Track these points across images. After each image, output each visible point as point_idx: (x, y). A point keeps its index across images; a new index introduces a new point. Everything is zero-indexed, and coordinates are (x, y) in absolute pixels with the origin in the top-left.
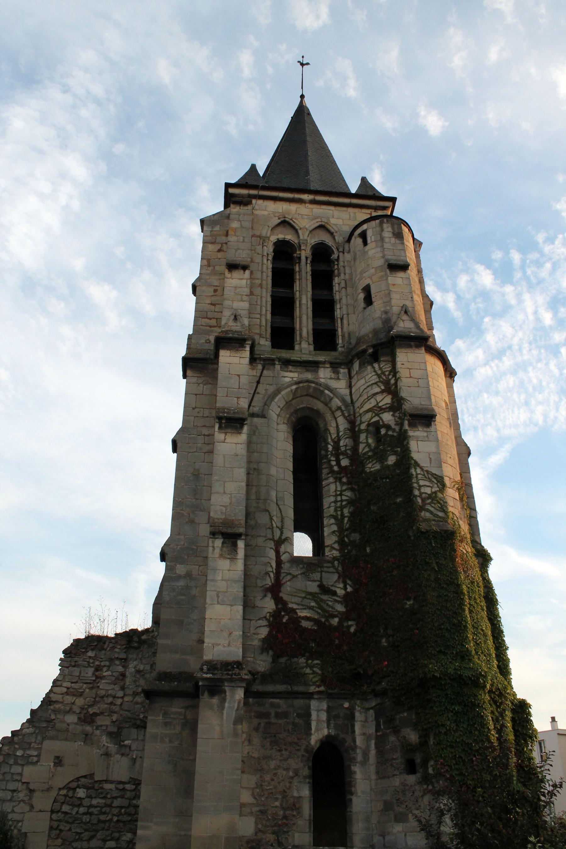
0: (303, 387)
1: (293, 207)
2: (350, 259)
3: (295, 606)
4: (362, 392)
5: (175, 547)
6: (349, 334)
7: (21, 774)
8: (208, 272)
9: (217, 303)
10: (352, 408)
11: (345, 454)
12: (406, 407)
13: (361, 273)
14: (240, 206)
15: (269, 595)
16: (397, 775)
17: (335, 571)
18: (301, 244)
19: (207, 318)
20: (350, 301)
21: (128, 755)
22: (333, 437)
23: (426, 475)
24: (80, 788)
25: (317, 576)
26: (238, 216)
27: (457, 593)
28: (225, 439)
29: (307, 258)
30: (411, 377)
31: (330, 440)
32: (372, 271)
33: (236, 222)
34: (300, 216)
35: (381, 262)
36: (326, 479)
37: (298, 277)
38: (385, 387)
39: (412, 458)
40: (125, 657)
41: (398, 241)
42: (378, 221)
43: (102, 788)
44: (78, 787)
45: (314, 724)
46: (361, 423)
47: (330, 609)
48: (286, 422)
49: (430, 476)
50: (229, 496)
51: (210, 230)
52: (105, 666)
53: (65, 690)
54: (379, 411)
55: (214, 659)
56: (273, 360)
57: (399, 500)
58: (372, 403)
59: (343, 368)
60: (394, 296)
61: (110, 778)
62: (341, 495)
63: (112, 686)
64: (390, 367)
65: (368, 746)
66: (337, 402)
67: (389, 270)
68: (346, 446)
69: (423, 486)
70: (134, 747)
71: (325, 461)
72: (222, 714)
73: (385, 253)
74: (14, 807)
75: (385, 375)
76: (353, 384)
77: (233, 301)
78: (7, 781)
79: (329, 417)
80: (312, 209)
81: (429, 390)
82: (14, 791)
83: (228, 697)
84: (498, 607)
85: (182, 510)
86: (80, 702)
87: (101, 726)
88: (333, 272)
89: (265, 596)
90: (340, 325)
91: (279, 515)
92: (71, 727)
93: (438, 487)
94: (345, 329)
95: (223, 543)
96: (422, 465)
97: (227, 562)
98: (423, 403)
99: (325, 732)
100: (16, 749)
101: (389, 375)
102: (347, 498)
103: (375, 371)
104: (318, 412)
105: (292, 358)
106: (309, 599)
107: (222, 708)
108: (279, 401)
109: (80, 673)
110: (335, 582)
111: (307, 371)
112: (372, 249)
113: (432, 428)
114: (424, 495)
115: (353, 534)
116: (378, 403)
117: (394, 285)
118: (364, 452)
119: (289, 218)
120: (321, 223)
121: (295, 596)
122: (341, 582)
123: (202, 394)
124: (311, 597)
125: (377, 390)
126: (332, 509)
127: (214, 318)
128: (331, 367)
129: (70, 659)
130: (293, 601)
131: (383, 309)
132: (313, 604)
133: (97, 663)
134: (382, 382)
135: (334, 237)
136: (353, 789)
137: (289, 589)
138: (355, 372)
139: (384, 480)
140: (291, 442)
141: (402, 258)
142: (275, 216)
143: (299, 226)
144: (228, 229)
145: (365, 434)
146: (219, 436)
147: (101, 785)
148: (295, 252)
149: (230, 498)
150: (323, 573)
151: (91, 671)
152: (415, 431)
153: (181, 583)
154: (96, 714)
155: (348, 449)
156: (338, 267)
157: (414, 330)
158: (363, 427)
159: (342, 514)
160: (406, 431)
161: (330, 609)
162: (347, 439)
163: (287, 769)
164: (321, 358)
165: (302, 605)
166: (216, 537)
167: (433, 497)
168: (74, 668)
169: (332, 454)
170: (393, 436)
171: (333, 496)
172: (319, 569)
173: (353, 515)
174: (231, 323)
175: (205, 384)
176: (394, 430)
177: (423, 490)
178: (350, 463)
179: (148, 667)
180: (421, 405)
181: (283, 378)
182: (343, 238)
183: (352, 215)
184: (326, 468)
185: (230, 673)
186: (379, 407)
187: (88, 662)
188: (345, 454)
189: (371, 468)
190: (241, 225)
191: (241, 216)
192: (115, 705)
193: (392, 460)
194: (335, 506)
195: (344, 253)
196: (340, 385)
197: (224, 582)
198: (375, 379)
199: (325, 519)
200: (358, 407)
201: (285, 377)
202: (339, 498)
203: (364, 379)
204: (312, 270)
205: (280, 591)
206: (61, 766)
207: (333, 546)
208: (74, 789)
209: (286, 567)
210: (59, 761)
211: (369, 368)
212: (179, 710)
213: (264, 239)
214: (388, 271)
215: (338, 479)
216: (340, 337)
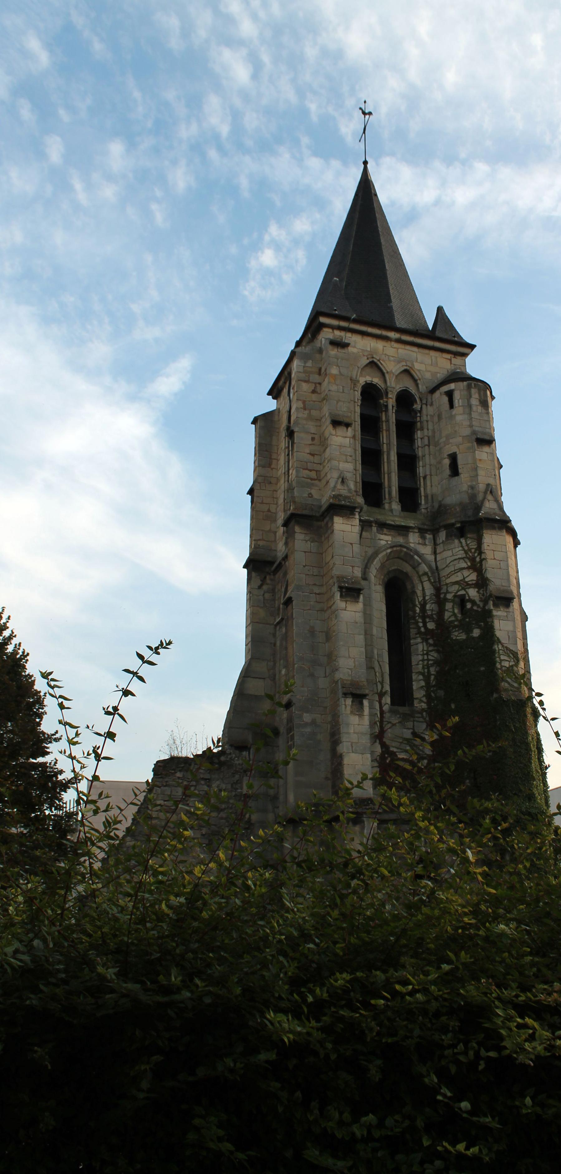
0: (396, 550)
1: (379, 345)
2: (432, 414)
3: (395, 750)
4: (449, 563)
5: (301, 698)
6: (432, 496)
8: (305, 416)
10: (437, 574)
11: (431, 617)
12: (491, 587)
13: (448, 437)
14: (338, 347)
15: (378, 741)
17: (423, 720)
18: (388, 391)
19: (307, 469)
20: (433, 462)
22: (420, 600)
23: (505, 650)
25: (410, 724)
26: (336, 360)
27: (527, 750)
28: (346, 607)
29: (393, 407)
30: (494, 559)
31: (417, 603)
32: (460, 439)
33: (335, 367)
34: (387, 357)
35: (467, 432)
36: (415, 638)
37: (384, 428)
38: (471, 564)
39: (496, 635)
40: (209, 777)
41: (484, 411)
42: (465, 383)
46: (448, 592)
47: (421, 753)
48: (381, 583)
49: (508, 652)
50: (353, 660)
51: (303, 365)
52: (192, 786)
54: (466, 586)
56: (371, 522)
57: (482, 669)
58: (458, 577)
59: (429, 534)
60: (481, 473)
62: (427, 654)
64: (475, 545)
66: (424, 568)
67: (477, 444)
68: (432, 610)
69: (503, 660)
71: (413, 621)
73: (474, 423)
75: (471, 552)
76: (438, 551)
77: (339, 461)
79: (416, 580)
80: (398, 349)
81: (508, 572)
84: (544, 754)
85: (303, 664)
88: (415, 423)
89: (375, 742)
90: (422, 484)
91: (380, 671)
93: (514, 661)
94: (429, 491)
95: (352, 702)
96: (503, 641)
97: (357, 718)
98: (504, 584)
101: (475, 552)
102: (433, 658)
103: (462, 546)
104: (406, 575)
105: (388, 522)
106: (405, 744)
108: (376, 563)
109: (171, 792)
110: (424, 730)
111: (399, 535)
112: (459, 415)
113: (511, 609)
114: (504, 668)
115: (439, 691)
116: (464, 578)
117: (480, 460)
118: (450, 620)
119: (376, 359)
120: (406, 368)
121: (395, 741)
122: (428, 729)
123: (311, 552)
124: (406, 742)
125: (464, 565)
126: (420, 666)
127: (314, 470)
128: (419, 532)
129: (161, 780)
130: (393, 745)
131: (469, 484)
132: (408, 748)
133: (185, 783)
134: (468, 559)
137: (389, 735)
138: (441, 541)
139: (470, 650)
140: (385, 602)
141: (487, 430)
142: (364, 356)
143: (386, 370)
144: (320, 366)
145: (451, 604)
146: (340, 603)
148: (382, 399)
149: (354, 662)
150: (415, 722)
152: (498, 611)
153: (308, 730)
155: (434, 614)
156: (420, 419)
157: (497, 511)
158: (450, 596)
159: (429, 671)
160: (490, 611)
161: (421, 753)
162: (433, 604)
164: (411, 523)
165: (401, 749)
166: (347, 696)
167: (510, 671)
168: (167, 788)
169: (419, 616)
170: (477, 611)
171: (421, 655)
172: (412, 719)
173: (438, 674)
174: (339, 486)
175: (312, 542)
176: (478, 606)
177: (503, 664)
178: (436, 627)
179: (229, 786)
180: (502, 586)
181: (379, 541)
182: (426, 387)
183: (434, 360)
184: (413, 628)
186: (466, 582)
188: (431, 617)
189: (457, 636)
190: (340, 372)
191: (339, 360)
193: (476, 633)
194: (423, 664)
195: (427, 405)
196: (426, 551)
198: (462, 554)
199: (413, 674)
200: (445, 576)
201: (381, 540)
202: (426, 657)
203: (451, 551)
204: (396, 420)
205: (384, 737)
207: (422, 699)
209: (387, 715)
211: (456, 541)
213: (354, 382)
214: (475, 444)
215: (425, 640)
216: (423, 498)
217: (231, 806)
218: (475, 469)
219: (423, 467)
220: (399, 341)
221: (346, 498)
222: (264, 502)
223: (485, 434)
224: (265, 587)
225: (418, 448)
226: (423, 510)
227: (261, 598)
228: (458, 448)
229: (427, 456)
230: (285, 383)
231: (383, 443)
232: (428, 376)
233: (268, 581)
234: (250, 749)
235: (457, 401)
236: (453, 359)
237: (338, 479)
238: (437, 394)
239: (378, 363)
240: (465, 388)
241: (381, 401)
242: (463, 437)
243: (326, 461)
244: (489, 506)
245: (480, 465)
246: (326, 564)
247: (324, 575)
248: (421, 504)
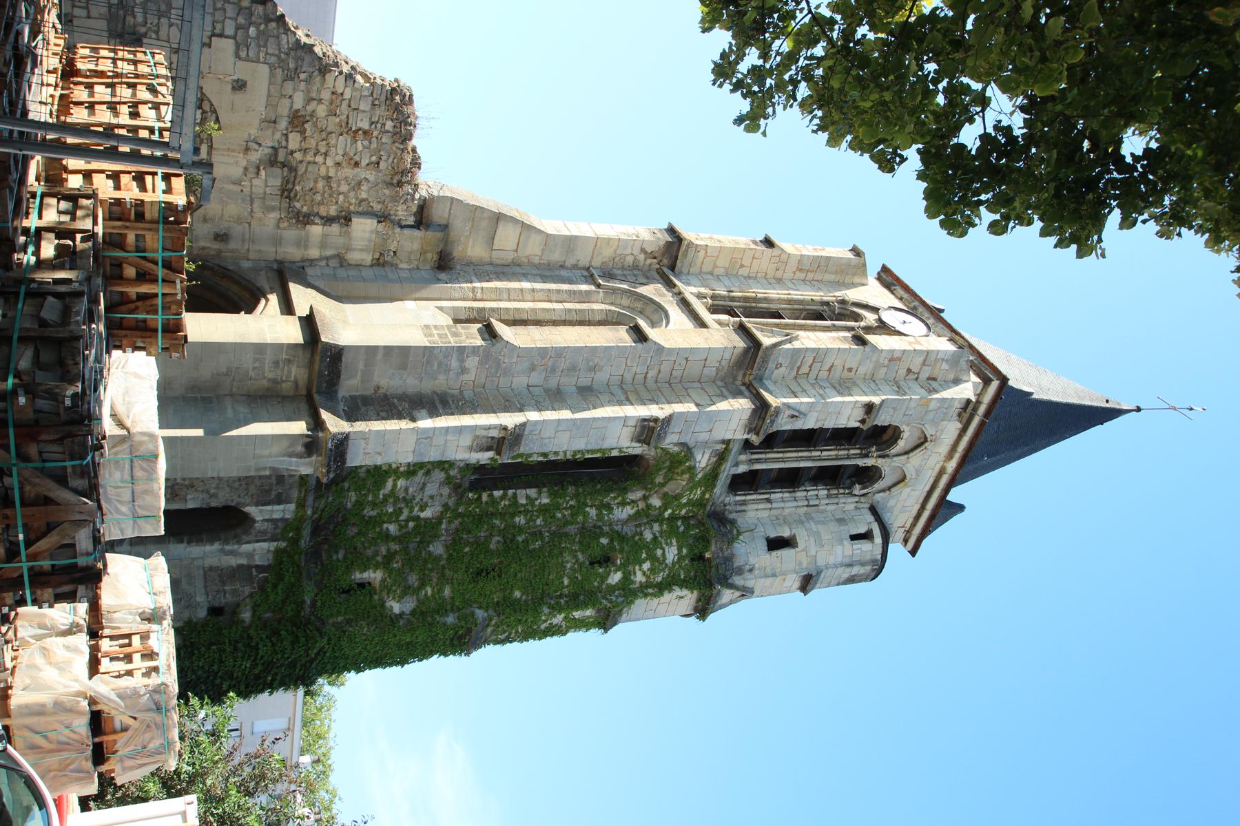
1: (944, 449)
6: (744, 511)
7: (221, 35)
9: (832, 373)
13: (817, 535)
16: (208, 597)
19: (814, 361)
20: (787, 512)
21: (246, 175)
24: (202, 114)
35: (821, 562)
41: (842, 580)
42: (879, 557)
44: (204, 112)
45: (269, 508)
53: (340, 91)
55: (349, 442)
60: (769, 581)
61: (214, 152)
63: (341, 152)
65: (240, 555)
70: (256, 182)
72: (284, 456)
78: (213, 15)
83: (303, 460)
85: (550, 357)
86: (321, 111)
87: (287, 140)
88: (837, 488)
92: (287, 102)
95: (493, 438)
99: (259, 518)
100: (257, 28)
107: (291, 455)
109: (364, 111)
117: (784, 580)
120: (908, 477)
131: (757, 566)
135: (883, 491)
136: (194, 544)
147: (205, 141)
148: (877, 450)
149: (549, 438)
151: (365, 125)
153: (454, 364)
154: (303, 132)
163: (217, 487)
175: (718, 369)
179: (364, 195)
185: (332, 463)
187: (378, 122)
192: (315, 155)
197: (443, 442)
201: (703, 455)
206: (234, 88)
210: (240, 86)
212: (293, 375)
217: (335, 196)
218: (774, 575)
219: (782, 498)
220: (942, 472)
221: (772, 422)
222: (754, 260)
223: (816, 583)
224: (642, 257)
225: (805, 490)
226: (728, 499)
227: (629, 251)
228: (803, 550)
229: (795, 504)
230: (901, 299)
231: (821, 451)
232: (891, 503)
233: (649, 261)
234: (419, 229)
235: (860, 546)
236: (904, 529)
237: (798, 411)
238: (871, 518)
239: (923, 447)
240: (873, 557)
241: (874, 449)
242: (816, 556)
243: (821, 392)
244: (727, 594)
245: (779, 579)
246: (686, 389)
247: (670, 384)
248: (736, 495)
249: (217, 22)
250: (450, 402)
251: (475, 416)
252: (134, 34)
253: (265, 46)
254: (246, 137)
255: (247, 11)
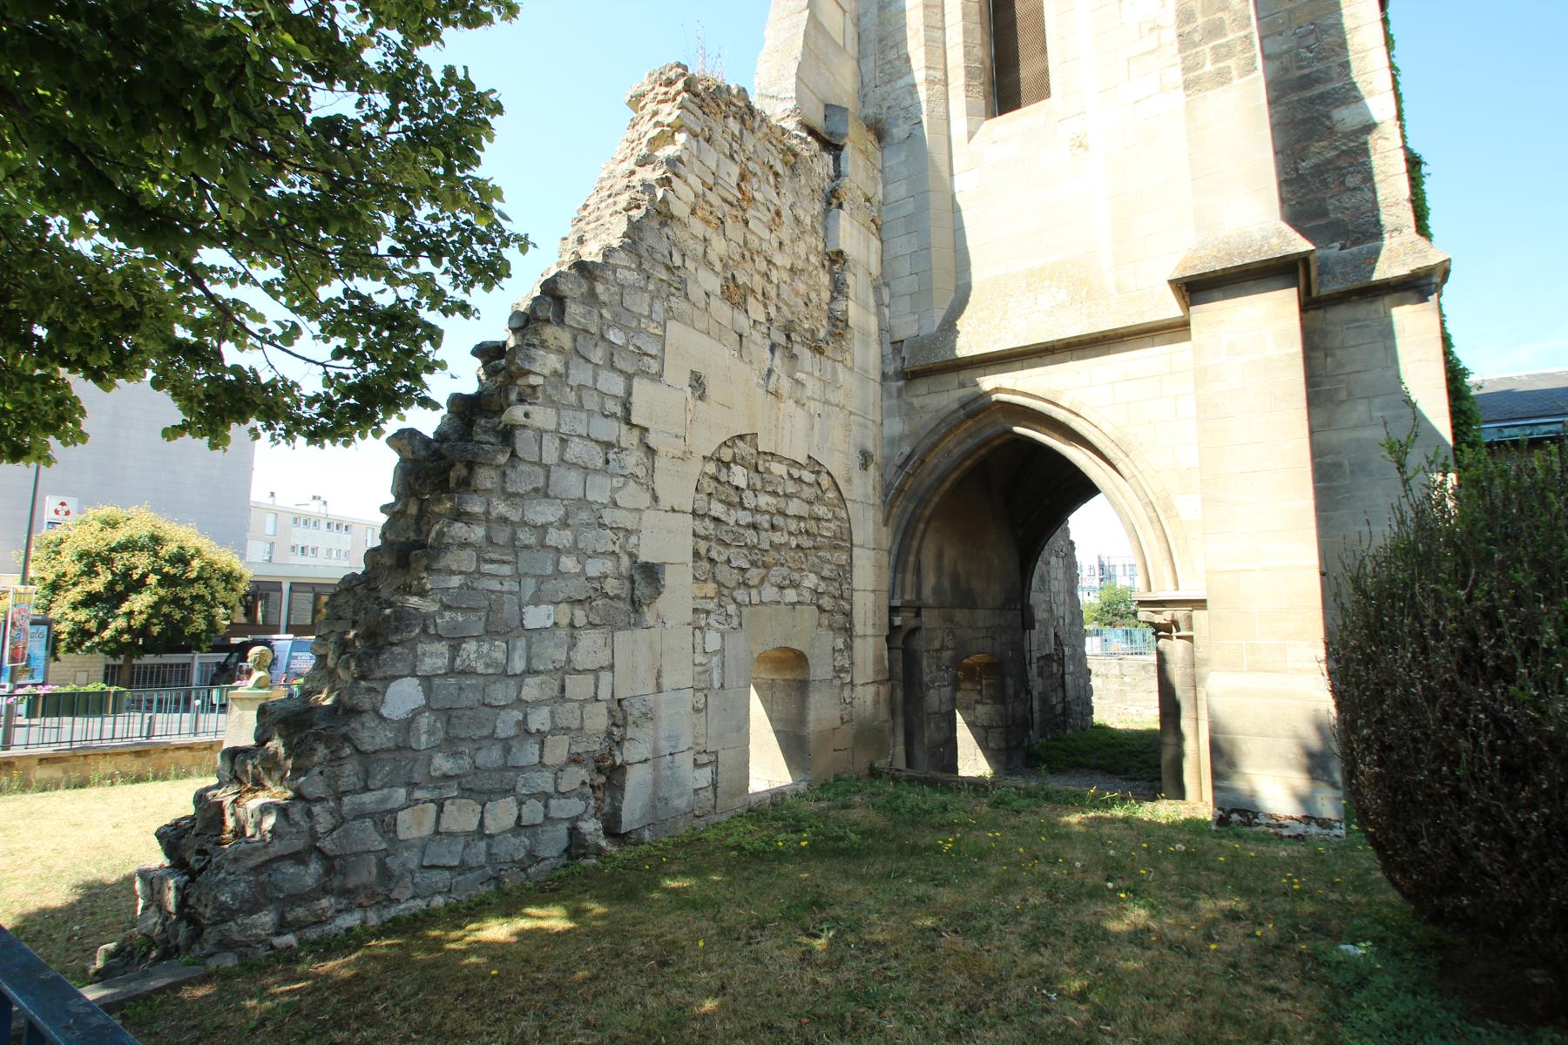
43: (768, 471)
74: (614, 490)
82: (608, 445)
208: (727, 465)
249: (603, 407)
250: (1306, 71)
251: (1348, 23)
252: (632, 581)
253: (638, 316)
254: (762, 392)
255: (580, 338)
